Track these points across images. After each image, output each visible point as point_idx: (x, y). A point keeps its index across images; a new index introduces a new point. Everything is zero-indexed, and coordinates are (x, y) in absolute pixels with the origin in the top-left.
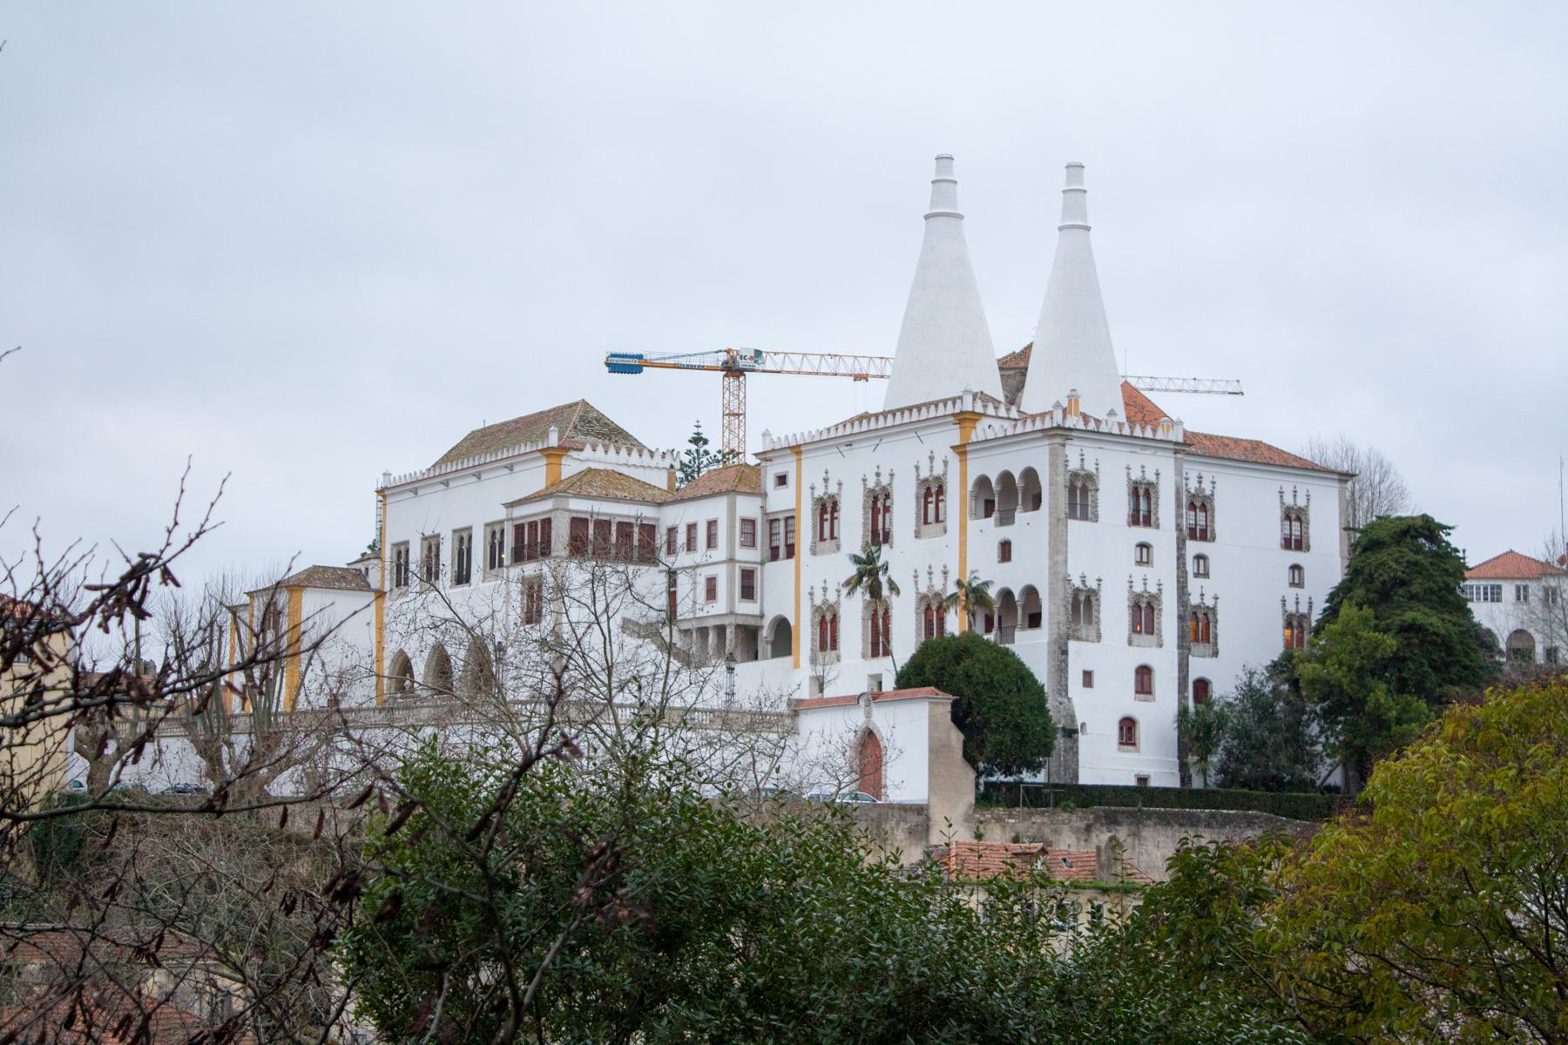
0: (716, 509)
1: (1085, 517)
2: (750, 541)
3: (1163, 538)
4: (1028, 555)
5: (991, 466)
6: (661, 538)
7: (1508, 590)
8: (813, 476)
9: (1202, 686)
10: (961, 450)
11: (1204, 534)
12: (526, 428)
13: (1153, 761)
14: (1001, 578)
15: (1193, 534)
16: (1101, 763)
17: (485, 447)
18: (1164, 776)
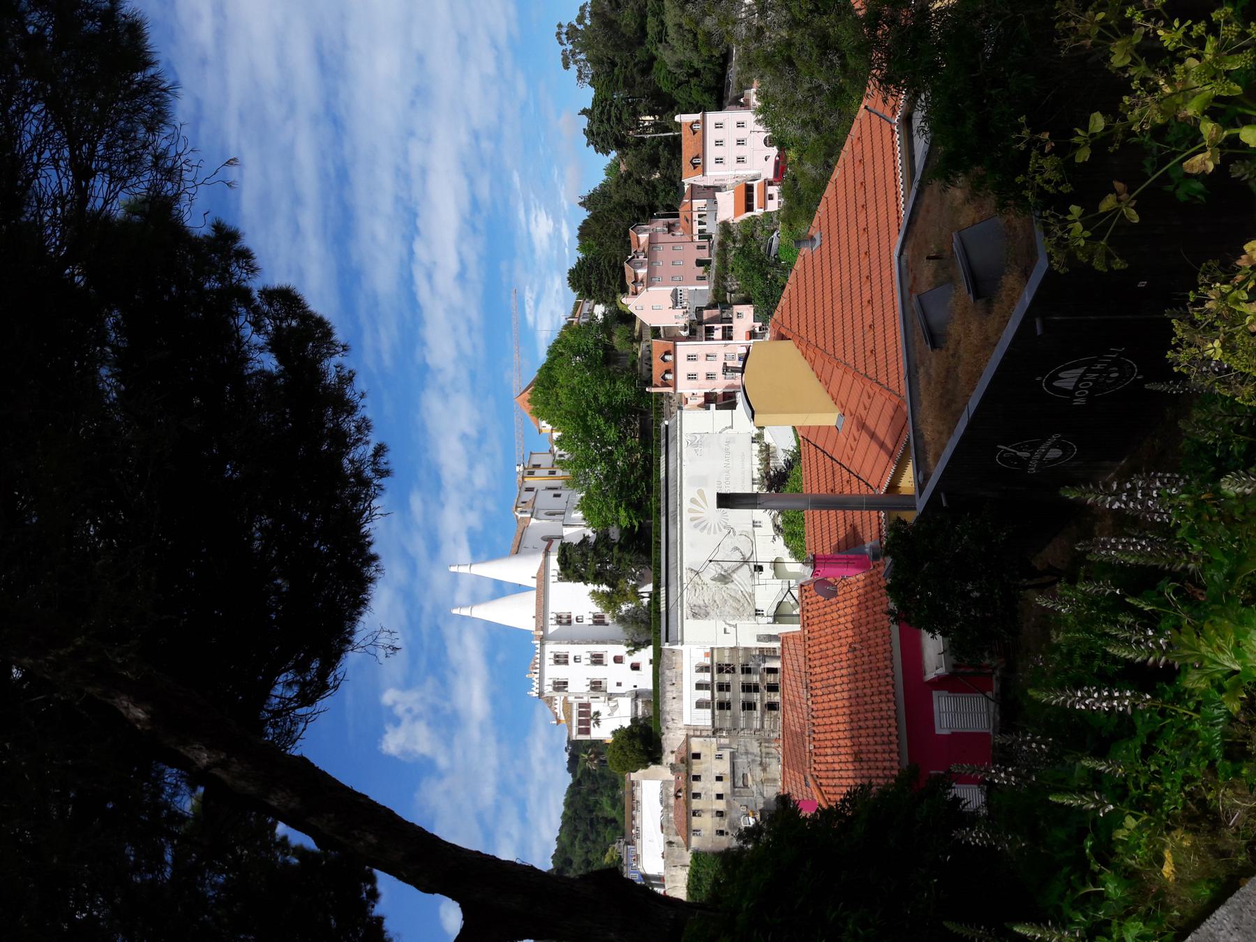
1: (566, 683)
13: (646, 654)
16: (644, 680)
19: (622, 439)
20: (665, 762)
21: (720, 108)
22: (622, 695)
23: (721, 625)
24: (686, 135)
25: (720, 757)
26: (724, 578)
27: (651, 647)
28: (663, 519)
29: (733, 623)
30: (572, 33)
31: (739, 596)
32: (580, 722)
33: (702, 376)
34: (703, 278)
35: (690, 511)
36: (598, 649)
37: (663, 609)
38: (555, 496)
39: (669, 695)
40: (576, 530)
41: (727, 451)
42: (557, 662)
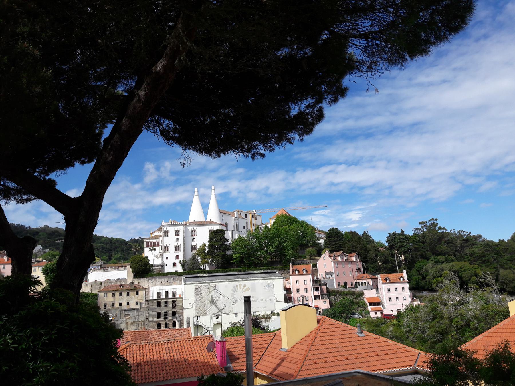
1: (167, 236)
16: (169, 269)
19: (269, 253)
20: (135, 280)
21: (411, 289)
22: (163, 260)
23: (193, 301)
24: (398, 275)
25: (137, 303)
26: (212, 301)
27: (183, 271)
28: (236, 273)
29: (194, 306)
30: (434, 225)
31: (205, 308)
32: (151, 243)
33: (298, 287)
34: (339, 285)
35: (241, 285)
36: (182, 249)
37: (199, 275)
38: (244, 227)
39: (163, 280)
40: (230, 236)
41: (267, 300)
42: (176, 232)
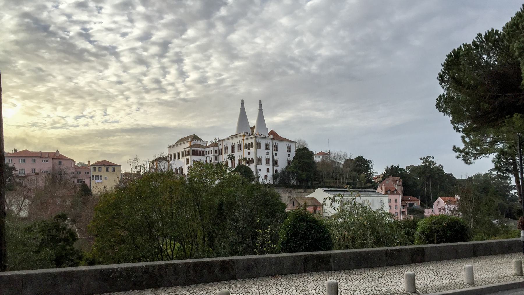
0: (212, 149)
2: (216, 152)
3: (270, 151)
4: (252, 153)
5: (247, 142)
6: (205, 153)
7: (321, 157)
8: (224, 144)
9: (276, 171)
10: (243, 140)
11: (277, 150)
12: (187, 138)
13: (269, 181)
14: (248, 157)
15: (275, 150)
17: (181, 141)
18: (271, 182)
